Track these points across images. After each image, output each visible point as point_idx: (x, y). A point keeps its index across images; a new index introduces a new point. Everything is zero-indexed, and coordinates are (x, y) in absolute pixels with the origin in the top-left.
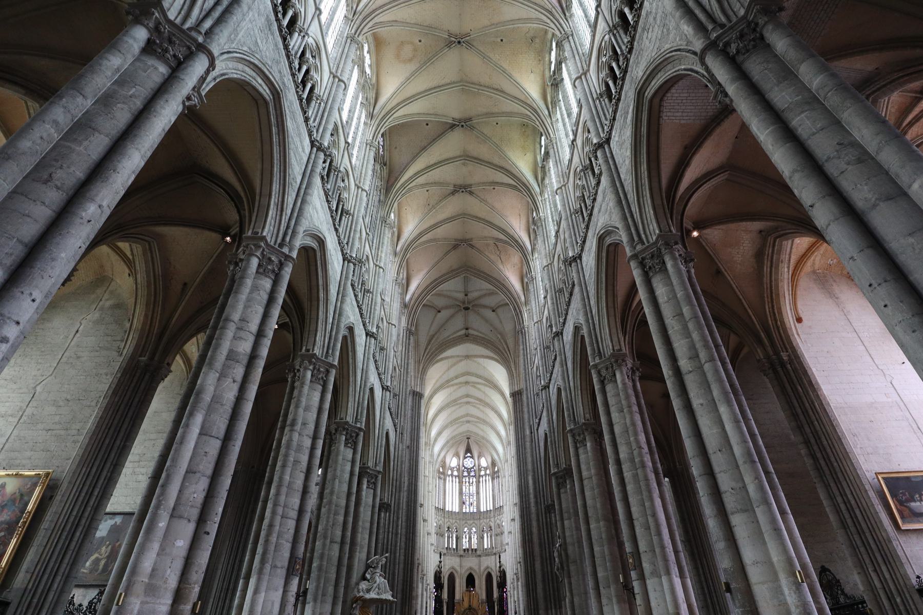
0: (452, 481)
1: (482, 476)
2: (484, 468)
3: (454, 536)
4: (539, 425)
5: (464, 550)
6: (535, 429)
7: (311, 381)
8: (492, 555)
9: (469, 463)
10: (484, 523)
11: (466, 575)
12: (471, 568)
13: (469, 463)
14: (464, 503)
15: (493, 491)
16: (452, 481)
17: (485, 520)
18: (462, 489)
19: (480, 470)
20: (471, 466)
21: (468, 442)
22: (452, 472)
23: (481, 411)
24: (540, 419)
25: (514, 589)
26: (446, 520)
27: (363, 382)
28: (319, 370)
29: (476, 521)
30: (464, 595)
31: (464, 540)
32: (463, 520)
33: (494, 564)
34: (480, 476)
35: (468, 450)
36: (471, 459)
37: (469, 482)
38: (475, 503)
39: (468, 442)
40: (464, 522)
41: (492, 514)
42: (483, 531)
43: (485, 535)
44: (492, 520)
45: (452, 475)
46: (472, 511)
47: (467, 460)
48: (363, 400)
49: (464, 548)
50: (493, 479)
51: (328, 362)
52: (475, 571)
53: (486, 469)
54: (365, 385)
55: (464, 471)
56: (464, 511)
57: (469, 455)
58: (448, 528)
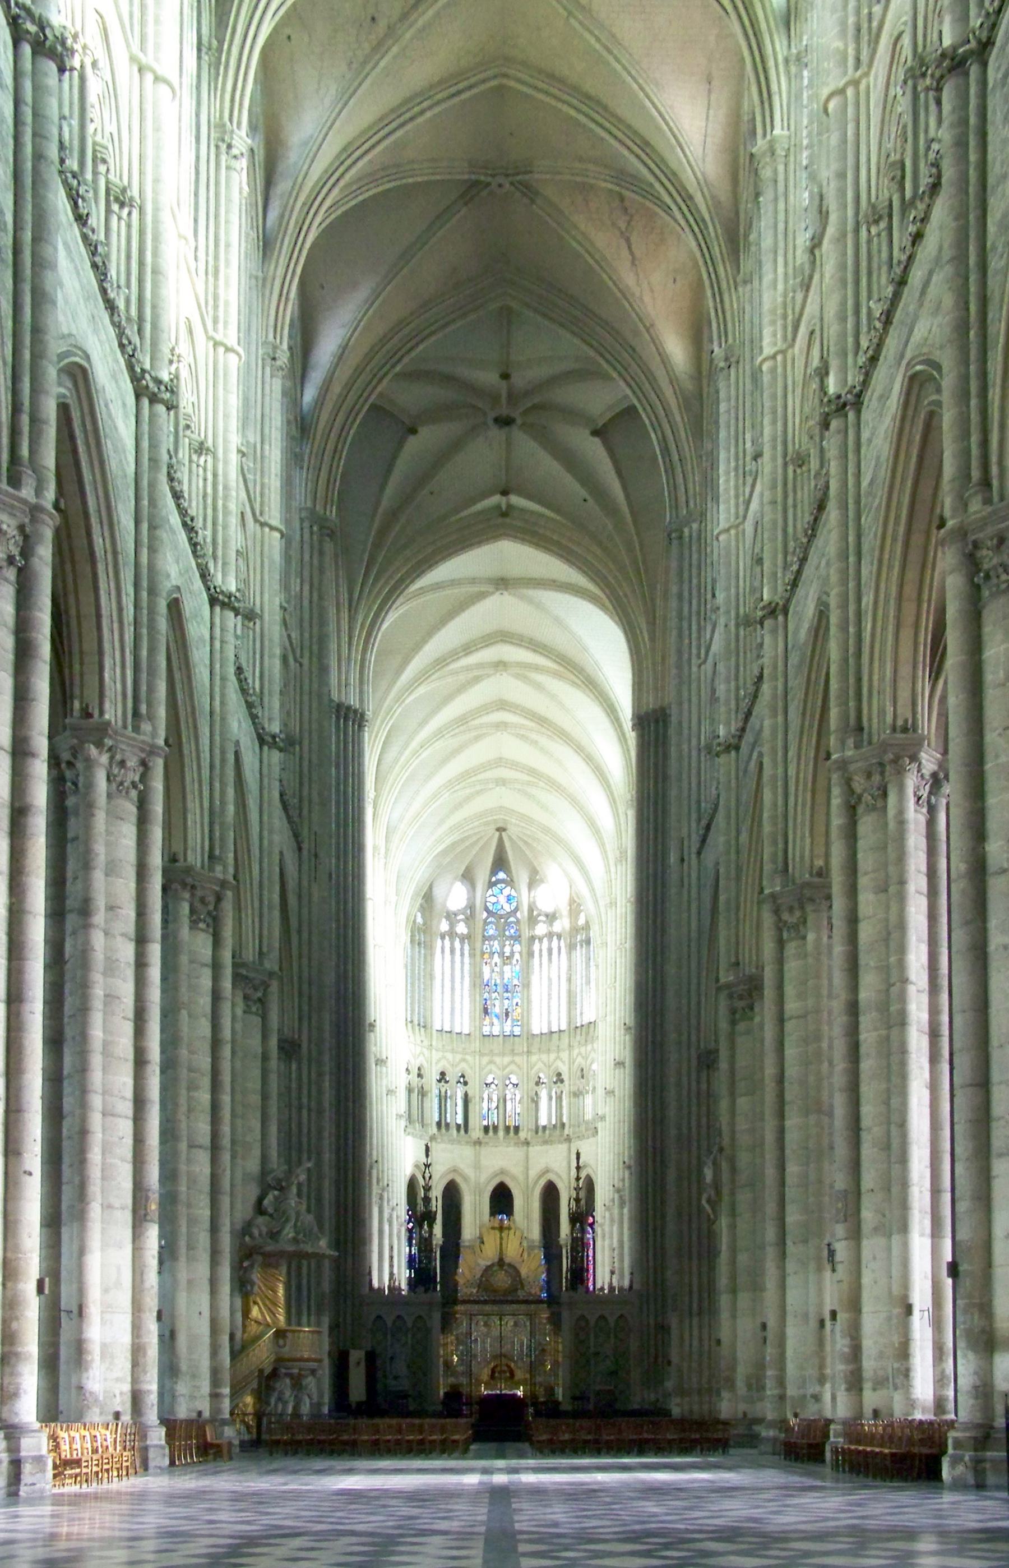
0: (452, 951)
1: (541, 940)
2: (547, 916)
3: (460, 1095)
4: (703, 841)
5: (486, 1129)
6: (694, 850)
7: (109, 796)
8: (560, 1142)
9: (502, 899)
10: (540, 1065)
11: (490, 1188)
12: (502, 1172)
13: (499, 899)
14: (486, 1011)
15: (569, 980)
16: (452, 951)
17: (544, 1057)
18: (481, 973)
19: (532, 920)
20: (507, 908)
21: (501, 841)
22: (452, 926)
23: (542, 749)
24: (708, 828)
25: (612, 1220)
26: (436, 1055)
27: (217, 751)
28: (122, 763)
29: (517, 1059)
30: (484, 1230)
31: (485, 1105)
32: (482, 1054)
33: (565, 1164)
34: (532, 938)
35: (500, 863)
36: (507, 891)
37: (501, 954)
38: (519, 1010)
39: (501, 841)
40: (485, 1060)
41: (565, 1041)
42: (538, 1083)
43: (544, 1094)
44: (565, 1055)
45: (452, 934)
46: (507, 1030)
47: (495, 890)
48: (223, 802)
49: (485, 1123)
50: (571, 947)
51: (143, 742)
52: (514, 1178)
53: (551, 918)
54: (223, 752)
55: (486, 923)
56: (486, 1030)
57: (501, 875)
58: (443, 1074)
